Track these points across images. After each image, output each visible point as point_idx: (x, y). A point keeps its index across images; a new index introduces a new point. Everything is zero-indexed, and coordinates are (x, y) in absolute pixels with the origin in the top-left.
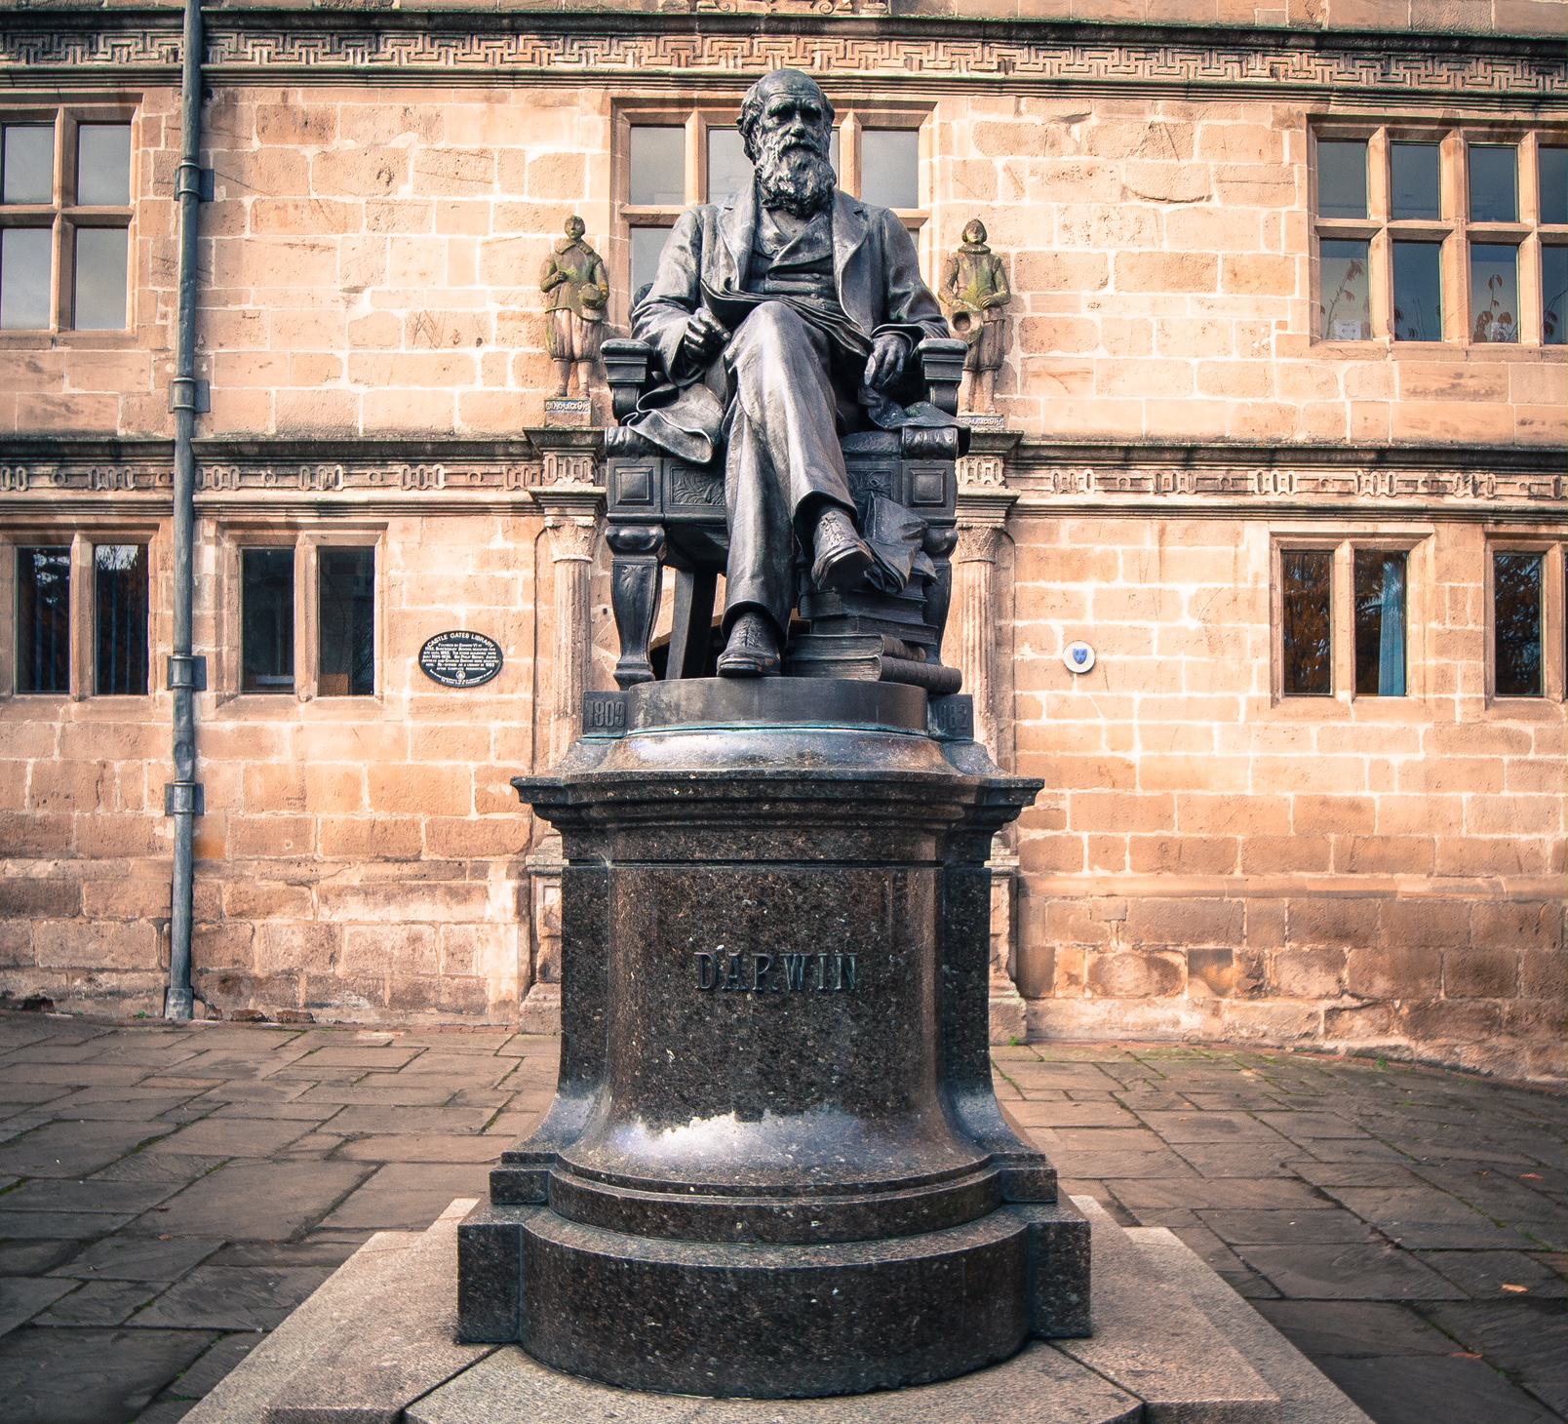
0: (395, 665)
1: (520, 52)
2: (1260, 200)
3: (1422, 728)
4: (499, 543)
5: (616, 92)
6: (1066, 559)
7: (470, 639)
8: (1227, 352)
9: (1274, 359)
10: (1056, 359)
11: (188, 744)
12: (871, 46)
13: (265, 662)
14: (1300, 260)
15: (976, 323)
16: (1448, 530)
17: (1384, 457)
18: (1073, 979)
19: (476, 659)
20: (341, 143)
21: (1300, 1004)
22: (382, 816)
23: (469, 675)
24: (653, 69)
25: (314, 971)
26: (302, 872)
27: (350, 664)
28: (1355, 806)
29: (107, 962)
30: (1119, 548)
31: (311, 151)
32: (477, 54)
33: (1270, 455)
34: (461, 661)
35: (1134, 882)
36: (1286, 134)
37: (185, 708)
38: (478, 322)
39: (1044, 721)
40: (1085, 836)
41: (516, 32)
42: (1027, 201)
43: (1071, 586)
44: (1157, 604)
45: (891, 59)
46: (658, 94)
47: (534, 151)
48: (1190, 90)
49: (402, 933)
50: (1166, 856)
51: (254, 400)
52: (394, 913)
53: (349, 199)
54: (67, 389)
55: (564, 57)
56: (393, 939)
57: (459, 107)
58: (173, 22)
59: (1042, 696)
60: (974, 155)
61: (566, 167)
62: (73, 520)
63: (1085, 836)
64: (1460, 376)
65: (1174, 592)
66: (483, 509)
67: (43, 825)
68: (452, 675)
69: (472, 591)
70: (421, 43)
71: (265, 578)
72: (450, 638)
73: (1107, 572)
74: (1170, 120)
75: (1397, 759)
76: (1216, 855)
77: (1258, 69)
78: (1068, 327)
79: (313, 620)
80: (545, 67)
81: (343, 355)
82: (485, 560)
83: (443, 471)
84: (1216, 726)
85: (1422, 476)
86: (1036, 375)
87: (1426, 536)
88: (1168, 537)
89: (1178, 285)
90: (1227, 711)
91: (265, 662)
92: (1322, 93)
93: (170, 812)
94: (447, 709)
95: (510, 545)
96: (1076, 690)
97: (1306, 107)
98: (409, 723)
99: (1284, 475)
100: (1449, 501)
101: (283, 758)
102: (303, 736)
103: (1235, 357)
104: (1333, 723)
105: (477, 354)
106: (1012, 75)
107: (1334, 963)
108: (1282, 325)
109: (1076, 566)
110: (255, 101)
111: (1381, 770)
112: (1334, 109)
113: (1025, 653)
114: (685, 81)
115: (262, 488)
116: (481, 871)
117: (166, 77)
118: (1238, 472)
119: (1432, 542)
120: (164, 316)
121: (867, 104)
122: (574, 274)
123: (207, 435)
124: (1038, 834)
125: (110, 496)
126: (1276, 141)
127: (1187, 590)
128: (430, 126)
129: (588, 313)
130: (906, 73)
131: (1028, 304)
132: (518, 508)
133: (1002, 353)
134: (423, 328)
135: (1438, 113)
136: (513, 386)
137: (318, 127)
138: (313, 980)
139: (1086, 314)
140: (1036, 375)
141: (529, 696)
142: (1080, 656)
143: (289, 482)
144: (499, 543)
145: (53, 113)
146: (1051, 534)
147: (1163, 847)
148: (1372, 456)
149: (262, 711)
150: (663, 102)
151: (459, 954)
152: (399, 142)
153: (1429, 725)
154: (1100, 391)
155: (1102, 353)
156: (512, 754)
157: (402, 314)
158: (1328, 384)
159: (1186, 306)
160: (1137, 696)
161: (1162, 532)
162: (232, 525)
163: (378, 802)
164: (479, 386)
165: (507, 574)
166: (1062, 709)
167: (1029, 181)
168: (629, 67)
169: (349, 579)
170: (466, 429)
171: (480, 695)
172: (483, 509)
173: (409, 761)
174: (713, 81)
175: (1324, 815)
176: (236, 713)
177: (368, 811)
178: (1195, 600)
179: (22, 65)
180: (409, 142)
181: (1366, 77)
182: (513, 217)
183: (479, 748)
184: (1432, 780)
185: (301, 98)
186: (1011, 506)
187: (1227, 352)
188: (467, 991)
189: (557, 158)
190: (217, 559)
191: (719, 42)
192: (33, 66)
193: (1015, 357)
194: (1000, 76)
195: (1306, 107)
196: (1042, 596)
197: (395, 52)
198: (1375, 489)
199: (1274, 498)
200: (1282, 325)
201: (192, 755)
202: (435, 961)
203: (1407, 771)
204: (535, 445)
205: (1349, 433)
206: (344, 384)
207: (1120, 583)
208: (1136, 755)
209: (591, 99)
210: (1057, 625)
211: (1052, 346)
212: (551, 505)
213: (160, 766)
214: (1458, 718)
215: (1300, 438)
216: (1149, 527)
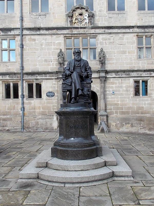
1: (54, 31)
2: (132, 44)
3: (149, 99)
4: (54, 82)
5: (65, 35)
6: (111, 82)
7: (51, 92)
8: (128, 60)
9: (133, 61)
10: (110, 62)
11: (23, 103)
12: (91, 30)
14: (136, 50)
15: (102, 59)
16: (152, 78)
17: (145, 71)
18: (113, 126)
19: (52, 94)
20: (37, 42)
21: (137, 128)
22: (43, 110)
23: (51, 96)
24: (68, 33)
25: (36, 126)
26: (35, 116)
27: (39, 95)
28: (143, 107)
29: (15, 126)
30: (117, 81)
31: (34, 42)
32: (50, 32)
33: (133, 71)
34: (50, 94)
35: (119, 116)
36: (134, 37)
37: (23, 100)
38: (51, 60)
39: (110, 99)
40: (114, 111)
41: (54, 29)
42: (107, 45)
43: (112, 85)
44: (121, 87)
45: (93, 31)
46: (69, 35)
47: (56, 42)
48: (124, 33)
49: (45, 122)
50: (123, 113)
52: (44, 120)
53: (38, 47)
54: (10, 67)
55: (59, 32)
56: (44, 123)
57: (48, 37)
58: (19, 29)
59: (109, 97)
60: (102, 41)
61: (60, 44)
62: (11, 81)
63: (114, 111)
64: (153, 62)
65: (123, 86)
66: (52, 79)
67: (8, 112)
68: (50, 96)
69: (51, 87)
70: (45, 31)
71: (30, 86)
72: (49, 92)
73: (116, 84)
74: (122, 36)
75: (147, 102)
76: (128, 113)
77: (131, 30)
78: (112, 58)
79: (35, 91)
80: (57, 33)
81: (38, 64)
82: (53, 84)
83: (48, 75)
84: (128, 99)
85: (149, 73)
86: (108, 64)
87: (149, 79)
88: (122, 80)
89: (123, 54)
90: (129, 98)
92: (138, 33)
93: (21, 110)
94: (49, 99)
95: (55, 83)
96: (113, 96)
97: (136, 34)
98: (45, 101)
99: (134, 73)
100: (152, 75)
101: (32, 105)
103: (129, 61)
104: (140, 99)
105: (51, 63)
106: (105, 32)
107: (140, 124)
108: (134, 57)
109: (113, 83)
110: (28, 37)
111: (145, 104)
112: (139, 34)
113: (108, 92)
114: (71, 34)
115: (30, 77)
116: (53, 116)
117: (18, 35)
118: (129, 73)
119: (150, 79)
120: (19, 60)
121: (90, 36)
122: (61, 54)
123: (24, 72)
124: (109, 111)
125: (14, 78)
126: (133, 38)
127: (124, 85)
128: (46, 40)
129: (63, 59)
130: (94, 33)
131: (107, 56)
132: (56, 79)
133: (105, 62)
134: (46, 61)
135: (150, 34)
136: (55, 66)
137: (34, 40)
138: (36, 127)
139: (113, 57)
140: (108, 64)
141: (57, 98)
142: (113, 93)
143: (33, 77)
144: (54, 82)
145: (7, 39)
146: (110, 80)
147: (122, 112)
148: (144, 71)
149: (31, 100)
150: (70, 36)
151: (51, 124)
152: (42, 41)
153: (150, 99)
154: (115, 65)
155: (115, 61)
156: (56, 104)
157: (43, 59)
158: (139, 63)
159: (124, 56)
160: (119, 96)
161: (122, 79)
162: (27, 81)
163: (42, 109)
164: (51, 66)
165: (55, 86)
166: (112, 98)
167: (107, 43)
168: (66, 33)
169: (39, 87)
170: (50, 71)
171: (52, 98)
172: (52, 79)
173: (45, 105)
174: (74, 34)
175: (139, 108)
176: (28, 100)
177: (41, 110)
178: (125, 86)
179: (4, 34)
180: (44, 41)
181: (143, 31)
182: (54, 49)
183: (52, 103)
184: (150, 104)
185: (32, 37)
186: (106, 77)
187: (128, 60)
188: (52, 128)
189: (59, 43)
190: (26, 85)
191: (75, 30)
192: (5, 34)
193: (106, 62)
194: (104, 32)
195: (136, 34)
196: (109, 86)
197: (42, 32)
198: (144, 74)
199: (133, 76)
200: (134, 57)
201: (23, 104)
202: (49, 125)
203: (148, 104)
204: (57, 73)
205: (141, 69)
206: (38, 66)
207: (117, 85)
208: (119, 103)
209: (62, 36)
210: (111, 89)
211: (110, 61)
212: (59, 78)
213: (20, 106)
214: (153, 98)
215: (136, 69)
216: (120, 79)
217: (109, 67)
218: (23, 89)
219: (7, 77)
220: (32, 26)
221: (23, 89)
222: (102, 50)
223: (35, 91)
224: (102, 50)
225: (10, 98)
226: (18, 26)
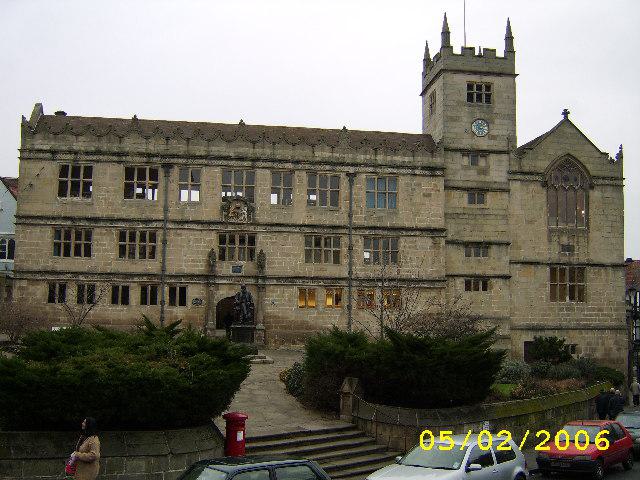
0: (189, 303)
11: (162, 312)
13: (172, 303)
27: (183, 303)
34: (197, 302)
35: (279, 330)
51: (171, 269)
71: (172, 291)
79: (179, 296)
91: (172, 303)
102: (179, 312)
109: (273, 291)
110: (172, 231)
137: (180, 235)
169: (183, 291)
175: (303, 323)
184: (316, 318)
190: (167, 289)
217: (268, 271)
218: (164, 293)
219: (145, 279)
220: (179, 217)
221: (164, 293)
222: (262, 251)
223: (179, 296)
224: (262, 251)
225: (89, 286)
226: (161, 217)
